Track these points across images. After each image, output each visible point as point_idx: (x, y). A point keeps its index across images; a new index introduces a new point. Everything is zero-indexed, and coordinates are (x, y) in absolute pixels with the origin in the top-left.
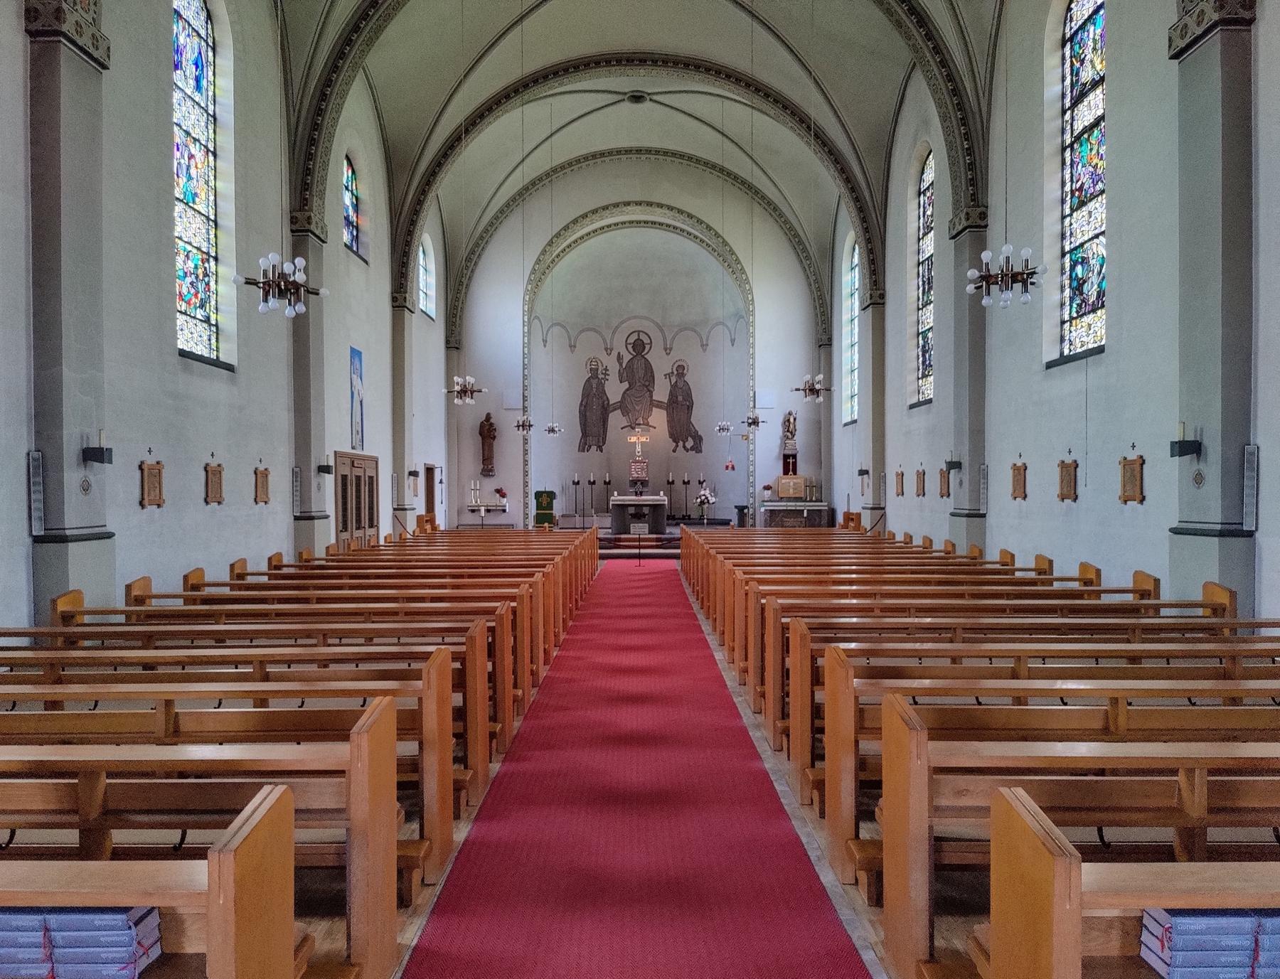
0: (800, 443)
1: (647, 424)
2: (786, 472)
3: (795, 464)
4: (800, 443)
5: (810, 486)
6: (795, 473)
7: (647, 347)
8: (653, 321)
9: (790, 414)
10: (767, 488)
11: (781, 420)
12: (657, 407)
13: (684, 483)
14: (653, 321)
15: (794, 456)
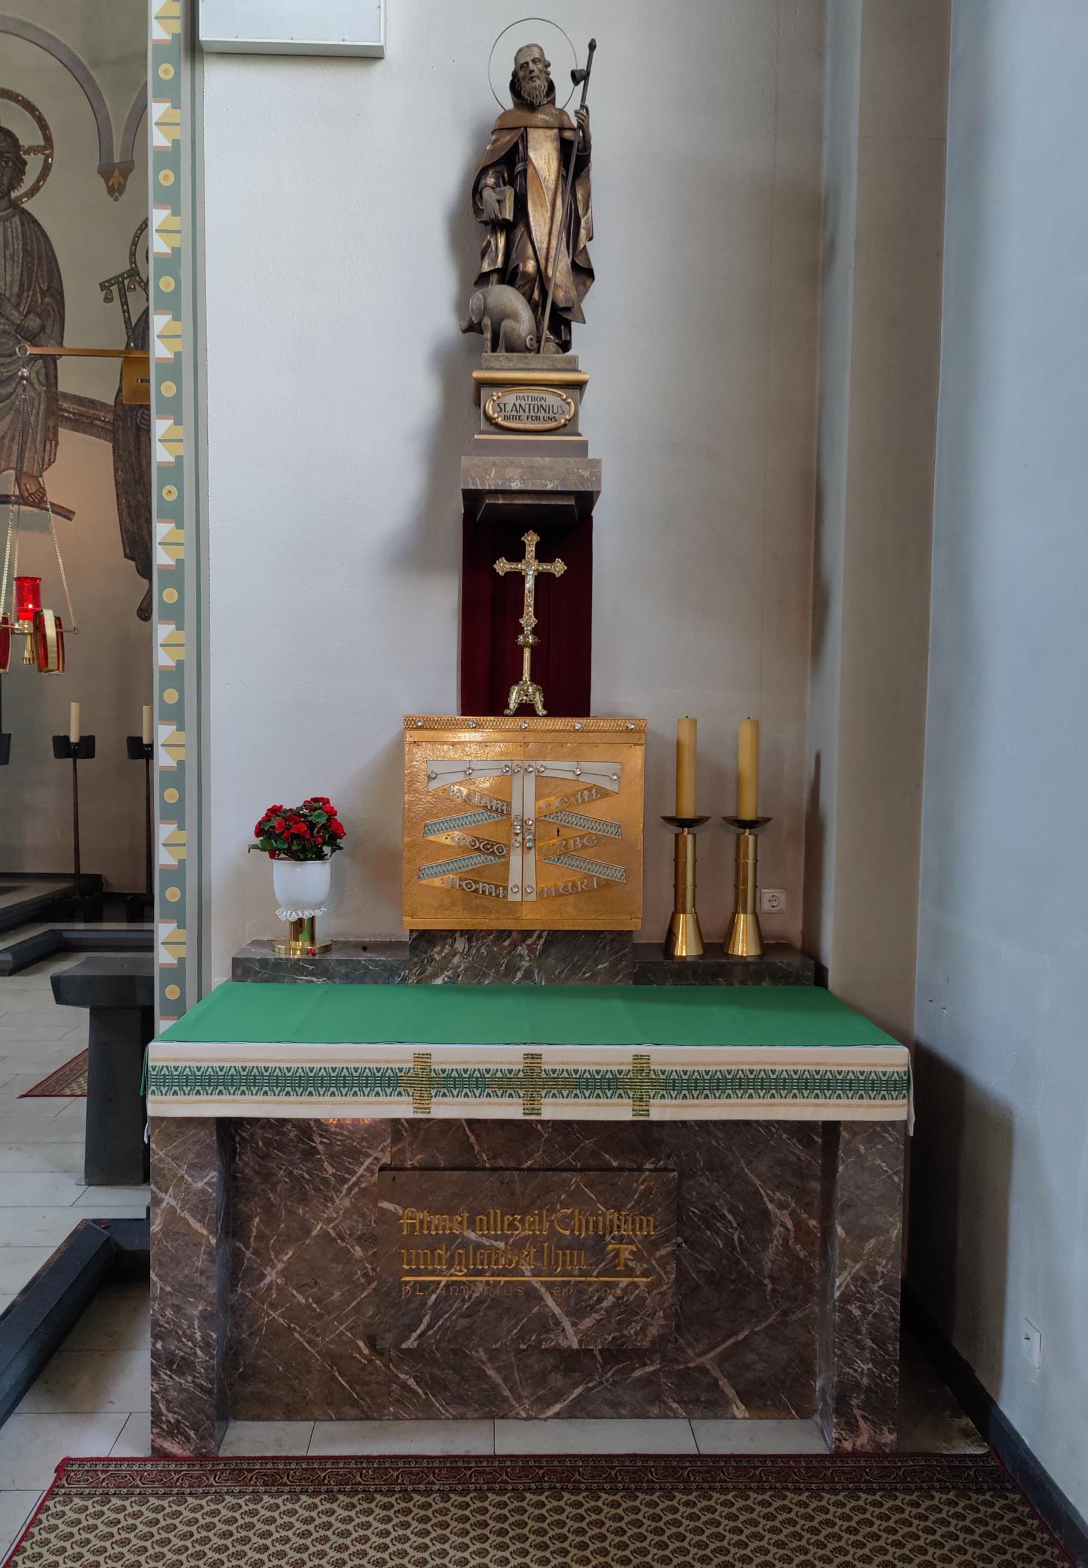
0: (630, 402)
1: (38, 500)
2: (483, 691)
3: (569, 605)
4: (630, 402)
5: (704, 824)
6: (568, 693)
7: (34, 165)
8: (50, 45)
9: (529, 86)
10: (298, 833)
11: (444, 168)
12: (80, 423)
13: (63, 747)
14: (50, 45)
15: (567, 524)
